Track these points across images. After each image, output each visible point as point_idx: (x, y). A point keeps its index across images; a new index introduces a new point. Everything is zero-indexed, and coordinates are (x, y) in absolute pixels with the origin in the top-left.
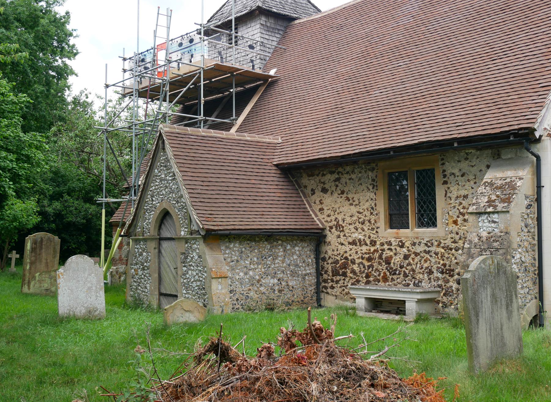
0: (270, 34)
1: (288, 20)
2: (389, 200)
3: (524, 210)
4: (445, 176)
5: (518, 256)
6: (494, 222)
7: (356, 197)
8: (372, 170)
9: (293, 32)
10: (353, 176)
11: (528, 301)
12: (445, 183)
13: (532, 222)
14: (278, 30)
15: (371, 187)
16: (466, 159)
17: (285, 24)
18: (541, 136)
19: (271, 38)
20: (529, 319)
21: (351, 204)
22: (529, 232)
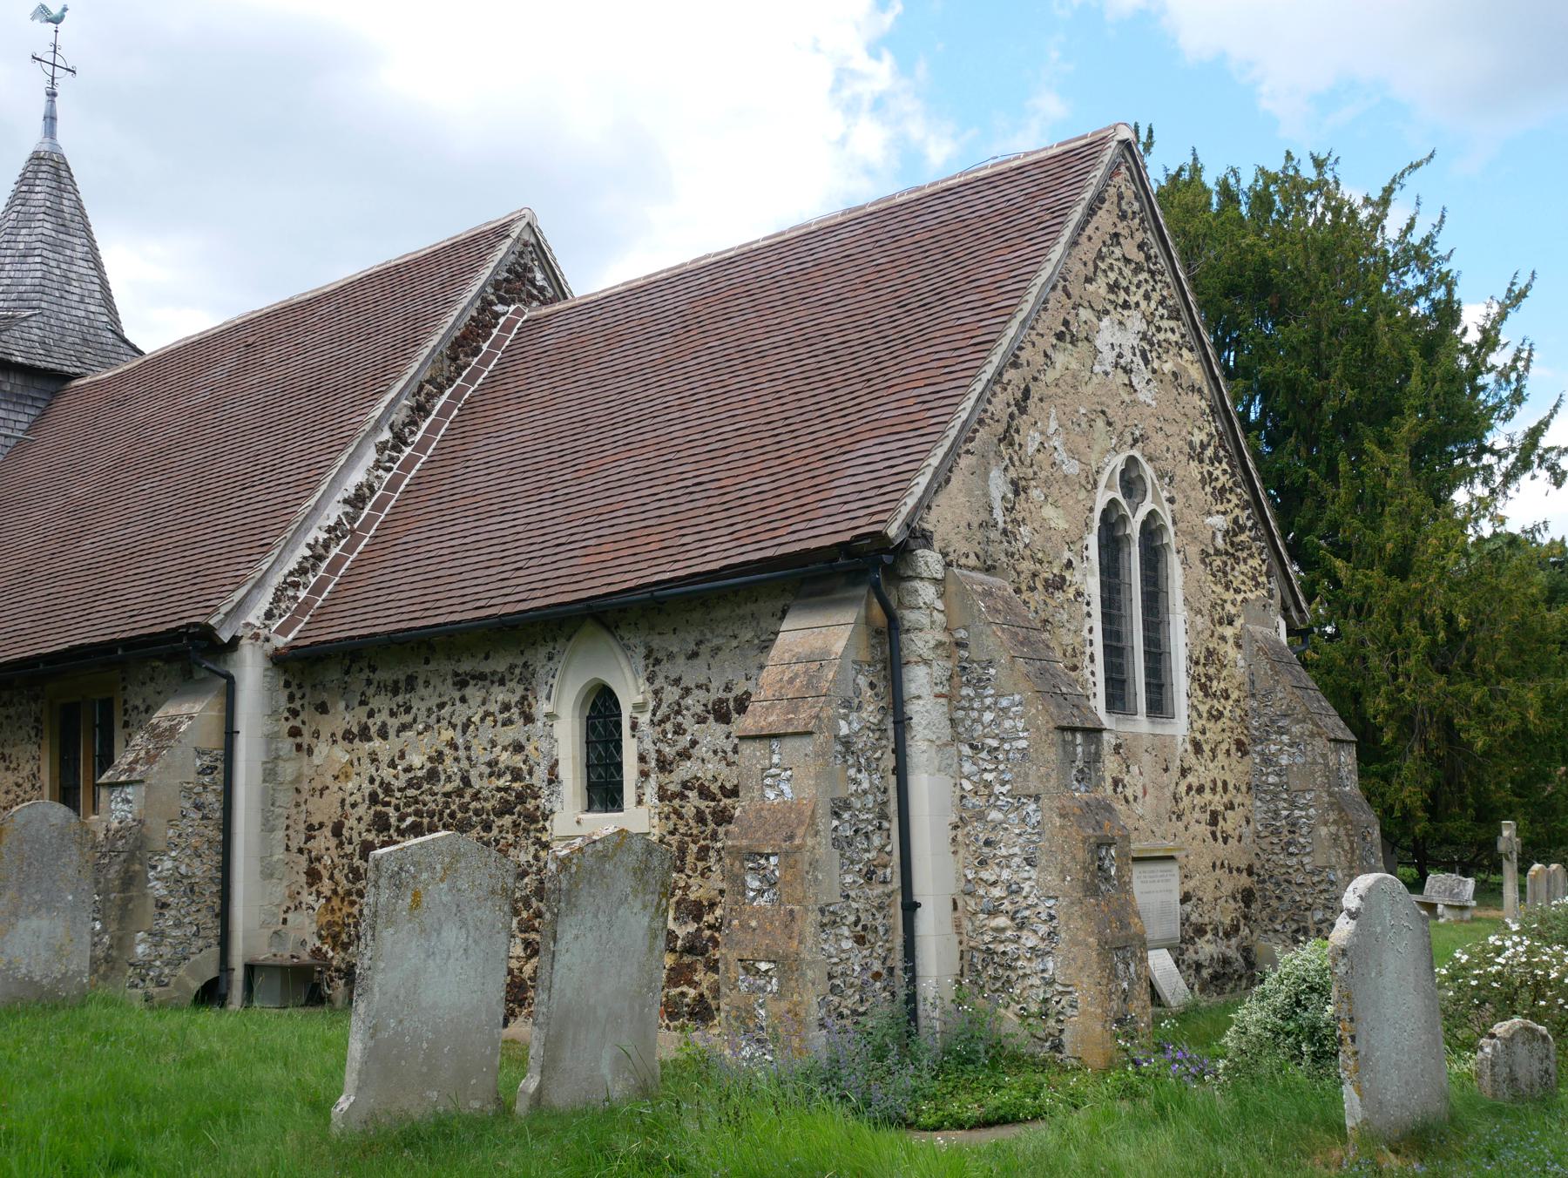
0: (10, 407)
1: (58, 379)
2: (61, 759)
3: (192, 777)
4: (126, 711)
5: (168, 864)
6: (129, 801)
7: (14, 751)
8: (36, 699)
9: (67, 409)
10: (12, 711)
11: (194, 950)
12: (126, 725)
13: (212, 799)
14: (34, 399)
15: (33, 734)
16: (152, 679)
17: (52, 387)
18: (235, 641)
19: (13, 416)
20: (195, 985)
21: (7, 769)
22: (204, 817)
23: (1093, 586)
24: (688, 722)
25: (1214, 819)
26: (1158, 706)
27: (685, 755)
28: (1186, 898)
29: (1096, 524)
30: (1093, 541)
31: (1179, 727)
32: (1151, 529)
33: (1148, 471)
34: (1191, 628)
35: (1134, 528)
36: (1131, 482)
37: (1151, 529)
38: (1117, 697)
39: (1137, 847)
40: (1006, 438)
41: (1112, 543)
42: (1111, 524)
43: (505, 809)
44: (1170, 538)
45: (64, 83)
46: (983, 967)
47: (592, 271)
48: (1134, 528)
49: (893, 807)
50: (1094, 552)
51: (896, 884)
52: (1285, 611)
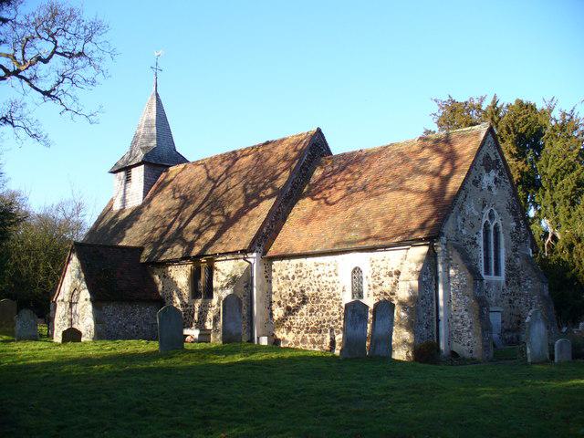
23: (481, 243)
24: (381, 277)
25: (511, 302)
26: (497, 273)
27: (381, 285)
28: (503, 322)
29: (483, 227)
30: (481, 232)
31: (502, 278)
32: (496, 228)
33: (495, 213)
34: (507, 254)
35: (492, 228)
36: (491, 216)
37: (496, 228)
38: (487, 272)
39: (491, 309)
40: (461, 209)
41: (486, 232)
42: (486, 226)
43: (330, 298)
44: (501, 229)
45: (159, 73)
46: (454, 335)
47: (337, 146)
48: (492, 228)
49: (434, 298)
50: (482, 235)
51: (435, 315)
52: (532, 247)
